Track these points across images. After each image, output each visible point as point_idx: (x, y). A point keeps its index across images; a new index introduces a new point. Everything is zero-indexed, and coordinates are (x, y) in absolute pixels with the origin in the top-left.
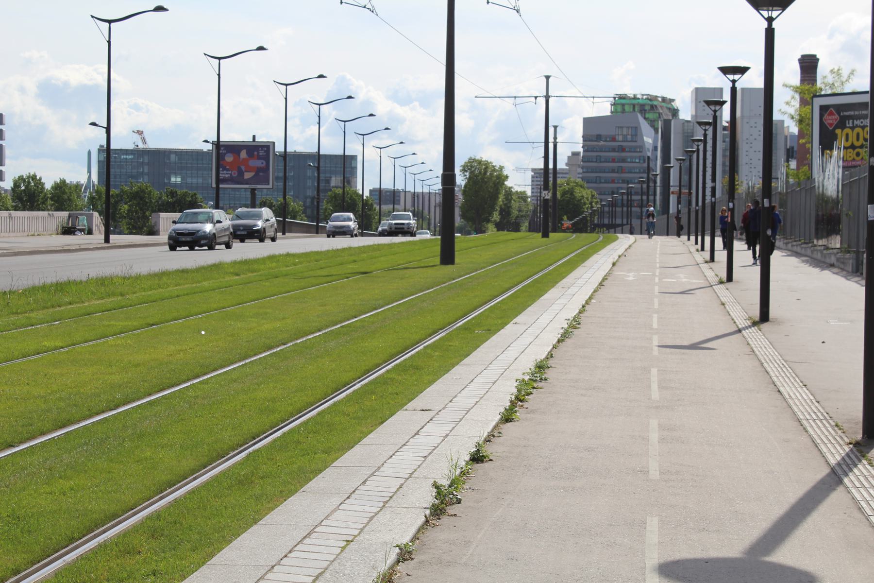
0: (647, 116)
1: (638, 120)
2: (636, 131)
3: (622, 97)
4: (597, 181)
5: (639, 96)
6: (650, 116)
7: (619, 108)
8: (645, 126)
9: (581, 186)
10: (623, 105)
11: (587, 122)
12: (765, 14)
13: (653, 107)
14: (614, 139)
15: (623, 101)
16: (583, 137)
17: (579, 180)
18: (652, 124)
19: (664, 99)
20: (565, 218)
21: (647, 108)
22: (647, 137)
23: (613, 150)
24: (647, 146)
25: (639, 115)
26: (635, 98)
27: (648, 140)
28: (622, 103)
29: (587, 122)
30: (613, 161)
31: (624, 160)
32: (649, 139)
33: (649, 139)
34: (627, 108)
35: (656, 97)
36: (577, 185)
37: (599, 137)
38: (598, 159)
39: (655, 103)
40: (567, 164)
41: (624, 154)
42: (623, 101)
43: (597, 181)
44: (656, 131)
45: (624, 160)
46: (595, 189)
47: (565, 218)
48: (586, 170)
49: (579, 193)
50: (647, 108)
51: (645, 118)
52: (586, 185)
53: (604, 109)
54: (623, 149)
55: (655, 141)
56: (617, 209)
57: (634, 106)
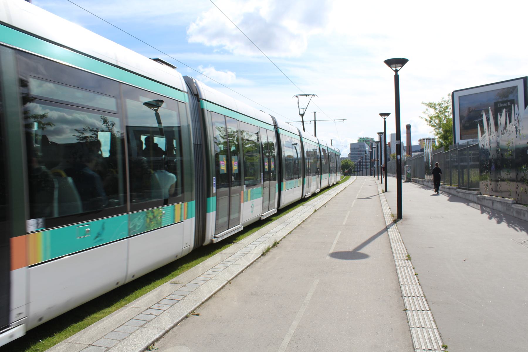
0: (367, 143)
1: (364, 144)
2: (364, 147)
3: (360, 138)
4: (355, 159)
5: (365, 138)
6: (368, 143)
7: (360, 141)
8: (366, 145)
9: (350, 161)
10: (361, 140)
11: (351, 145)
12: (384, 117)
13: (368, 141)
14: (358, 149)
15: (360, 139)
16: (351, 148)
17: (350, 160)
18: (368, 145)
19: (371, 139)
20: (346, 169)
21: (367, 141)
22: (367, 148)
23: (358, 152)
24: (367, 150)
25: (365, 142)
26: (364, 138)
27: (367, 149)
28: (361, 140)
29: (351, 145)
30: (358, 154)
31: (361, 154)
32: (368, 148)
33: (368, 148)
34: (362, 141)
35: (369, 138)
36: (349, 161)
37: (354, 149)
38: (354, 154)
39: (369, 139)
40: (348, 156)
41: (361, 153)
42: (360, 139)
43: (355, 159)
44: (369, 146)
45: (361, 154)
46: (354, 162)
47: (346, 169)
48: (351, 157)
49: (349, 163)
50: (367, 141)
51: (367, 143)
52: (351, 161)
53: (356, 141)
54: (361, 151)
55: (369, 149)
56: (363, 167)
57: (363, 140)
